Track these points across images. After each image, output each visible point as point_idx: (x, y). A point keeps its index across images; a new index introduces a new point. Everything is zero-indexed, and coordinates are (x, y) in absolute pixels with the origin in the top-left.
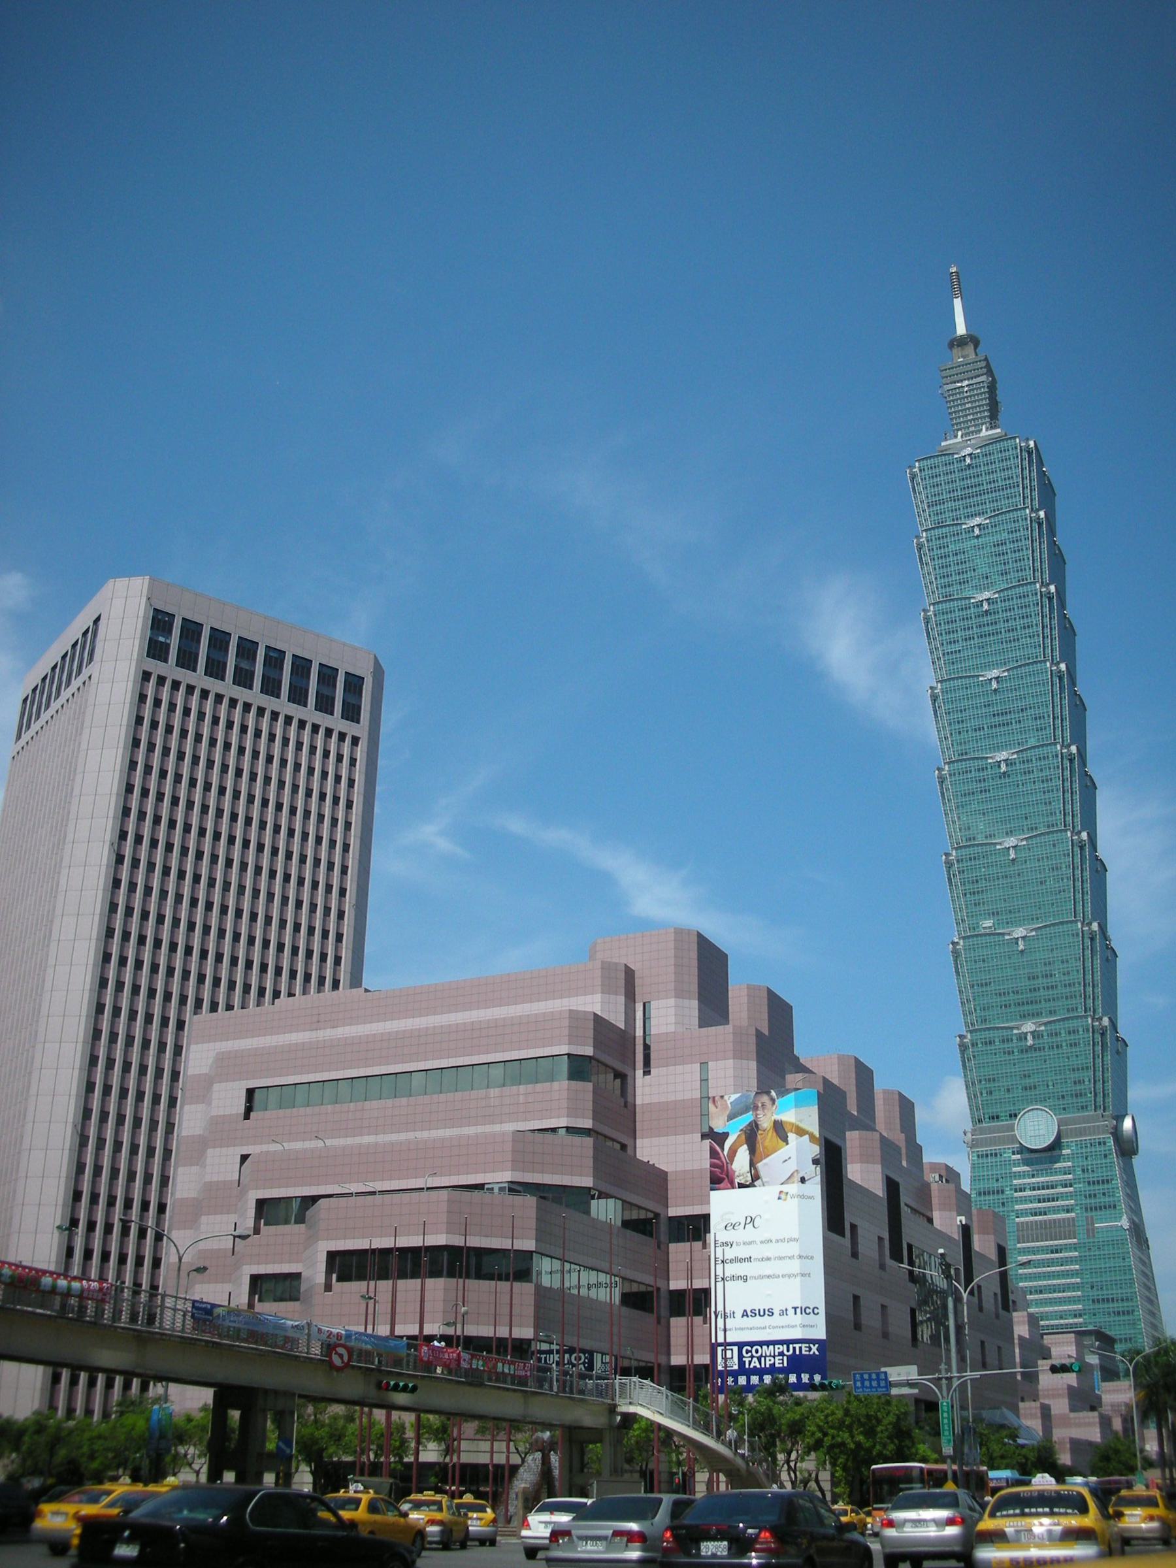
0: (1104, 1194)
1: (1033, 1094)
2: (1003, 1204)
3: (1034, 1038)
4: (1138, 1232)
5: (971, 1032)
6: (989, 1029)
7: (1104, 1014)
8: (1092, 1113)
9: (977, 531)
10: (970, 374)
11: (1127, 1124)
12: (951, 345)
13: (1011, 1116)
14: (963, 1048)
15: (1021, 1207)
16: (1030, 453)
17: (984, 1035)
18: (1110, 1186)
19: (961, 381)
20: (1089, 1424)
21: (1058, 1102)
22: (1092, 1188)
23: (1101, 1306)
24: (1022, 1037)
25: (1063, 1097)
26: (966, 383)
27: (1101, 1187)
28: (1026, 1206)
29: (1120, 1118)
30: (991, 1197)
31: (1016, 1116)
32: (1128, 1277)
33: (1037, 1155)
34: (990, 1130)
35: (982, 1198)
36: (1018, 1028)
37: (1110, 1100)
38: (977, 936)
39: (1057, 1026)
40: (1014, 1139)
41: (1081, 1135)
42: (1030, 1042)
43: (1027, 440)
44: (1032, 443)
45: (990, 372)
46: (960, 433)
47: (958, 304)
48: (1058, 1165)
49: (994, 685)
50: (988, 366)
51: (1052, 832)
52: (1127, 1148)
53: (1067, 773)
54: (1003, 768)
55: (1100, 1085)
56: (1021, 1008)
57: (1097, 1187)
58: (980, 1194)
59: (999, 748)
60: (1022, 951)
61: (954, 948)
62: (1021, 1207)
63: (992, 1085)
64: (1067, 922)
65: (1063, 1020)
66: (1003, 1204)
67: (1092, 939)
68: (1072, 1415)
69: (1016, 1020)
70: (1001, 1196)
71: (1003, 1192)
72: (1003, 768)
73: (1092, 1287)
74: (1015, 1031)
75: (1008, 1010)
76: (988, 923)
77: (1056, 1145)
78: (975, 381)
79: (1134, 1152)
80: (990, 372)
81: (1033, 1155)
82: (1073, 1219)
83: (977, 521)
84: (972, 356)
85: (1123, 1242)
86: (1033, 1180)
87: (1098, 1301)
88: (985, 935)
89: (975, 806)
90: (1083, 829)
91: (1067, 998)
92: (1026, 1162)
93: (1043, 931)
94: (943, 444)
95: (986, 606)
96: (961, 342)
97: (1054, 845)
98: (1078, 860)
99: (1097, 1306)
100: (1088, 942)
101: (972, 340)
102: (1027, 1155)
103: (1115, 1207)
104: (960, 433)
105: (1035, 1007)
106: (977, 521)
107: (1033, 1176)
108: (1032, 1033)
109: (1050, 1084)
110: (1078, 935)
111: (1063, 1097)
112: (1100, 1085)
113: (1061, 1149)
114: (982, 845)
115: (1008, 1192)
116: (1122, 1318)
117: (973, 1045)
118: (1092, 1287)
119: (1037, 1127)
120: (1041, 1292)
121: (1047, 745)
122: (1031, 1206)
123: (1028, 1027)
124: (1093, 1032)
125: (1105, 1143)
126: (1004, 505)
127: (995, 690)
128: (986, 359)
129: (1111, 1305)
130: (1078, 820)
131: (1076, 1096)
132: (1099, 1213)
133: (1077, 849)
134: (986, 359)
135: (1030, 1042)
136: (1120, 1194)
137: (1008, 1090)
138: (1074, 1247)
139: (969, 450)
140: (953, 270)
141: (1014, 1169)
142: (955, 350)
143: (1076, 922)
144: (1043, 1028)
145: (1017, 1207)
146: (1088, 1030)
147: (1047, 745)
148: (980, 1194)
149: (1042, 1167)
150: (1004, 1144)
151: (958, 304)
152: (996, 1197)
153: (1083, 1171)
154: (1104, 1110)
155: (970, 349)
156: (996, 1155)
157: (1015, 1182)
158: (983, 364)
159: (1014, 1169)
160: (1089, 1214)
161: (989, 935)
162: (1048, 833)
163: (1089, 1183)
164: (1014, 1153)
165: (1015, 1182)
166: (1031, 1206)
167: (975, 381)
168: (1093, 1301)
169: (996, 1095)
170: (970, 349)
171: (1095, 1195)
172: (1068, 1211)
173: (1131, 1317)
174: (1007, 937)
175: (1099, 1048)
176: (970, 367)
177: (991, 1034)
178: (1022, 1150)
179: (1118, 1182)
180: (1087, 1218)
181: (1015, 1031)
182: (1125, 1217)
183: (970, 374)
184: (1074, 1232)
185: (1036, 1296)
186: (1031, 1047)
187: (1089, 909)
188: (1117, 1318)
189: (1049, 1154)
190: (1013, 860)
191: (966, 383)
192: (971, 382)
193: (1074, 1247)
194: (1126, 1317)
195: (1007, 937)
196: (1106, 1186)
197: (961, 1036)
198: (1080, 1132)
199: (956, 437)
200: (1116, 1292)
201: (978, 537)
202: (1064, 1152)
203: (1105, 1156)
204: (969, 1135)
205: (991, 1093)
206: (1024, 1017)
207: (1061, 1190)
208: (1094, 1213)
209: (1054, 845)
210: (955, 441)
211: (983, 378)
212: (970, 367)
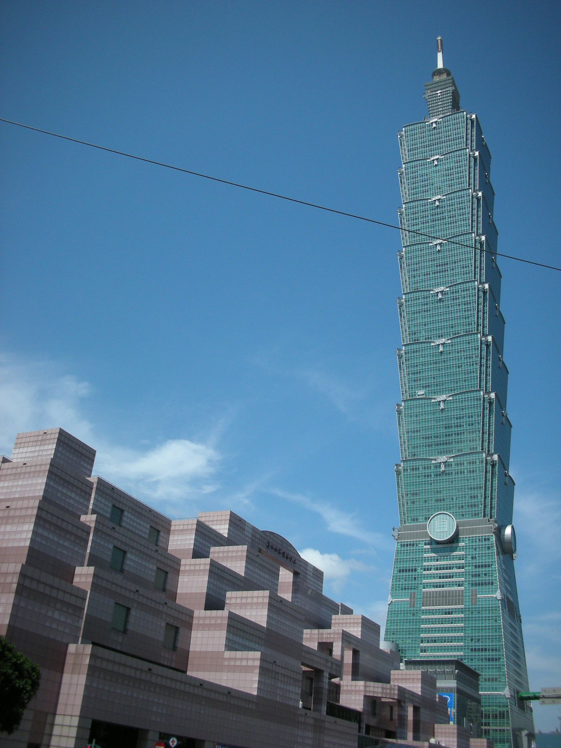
0: (485, 574)
1: (441, 504)
2: (415, 578)
3: (445, 466)
4: (511, 606)
5: (404, 461)
6: (415, 460)
7: (495, 453)
8: (482, 518)
9: (436, 163)
10: (443, 87)
11: (508, 531)
12: (434, 74)
13: (426, 519)
14: (398, 473)
15: (427, 581)
16: (472, 121)
17: (412, 464)
18: (490, 569)
19: (437, 91)
20: (247, 669)
21: (459, 510)
22: (477, 570)
23: (477, 654)
24: (438, 466)
25: (462, 507)
26: (440, 91)
27: (484, 569)
28: (430, 581)
30: (407, 574)
31: (429, 518)
32: (498, 634)
33: (441, 546)
34: (411, 528)
35: (401, 574)
36: (435, 460)
37: (495, 511)
38: (413, 400)
39: (462, 458)
40: (426, 534)
41: (473, 534)
42: (443, 468)
43: (471, 113)
44: (474, 116)
45: (454, 84)
47: (440, 56)
49: (438, 248)
53: (481, 300)
54: (440, 296)
55: (488, 500)
56: (439, 447)
57: (481, 569)
58: (400, 571)
59: (438, 285)
60: (442, 410)
61: (398, 408)
62: (427, 581)
64: (473, 391)
65: (466, 454)
66: (415, 578)
67: (491, 404)
68: (227, 654)
69: (435, 455)
70: (414, 573)
71: (416, 570)
72: (440, 296)
73: (472, 640)
74: (433, 462)
75: (430, 449)
76: (421, 392)
77: (454, 540)
78: (445, 90)
80: (454, 84)
81: (439, 546)
82: (462, 591)
83: (437, 157)
85: (496, 609)
86: (437, 563)
87: (475, 650)
88: (419, 399)
89: (420, 321)
90: (489, 335)
91: (470, 441)
92: (433, 551)
93: (457, 397)
95: (437, 203)
96: (439, 72)
97: (469, 343)
98: (484, 353)
99: (473, 653)
100: (487, 405)
101: (445, 71)
102: (435, 546)
103: (492, 584)
105: (448, 446)
106: (437, 157)
107: (437, 560)
108: (444, 463)
109: (454, 498)
110: (480, 399)
111: (462, 507)
112: (488, 500)
113: (458, 542)
114: (422, 343)
115: (419, 570)
116: (491, 663)
117: (404, 470)
118: (472, 640)
119: (442, 527)
120: (435, 641)
121: (468, 282)
122: (434, 581)
123: (443, 458)
124: (486, 464)
125: (489, 539)
126: (455, 148)
127: (439, 251)
128: (453, 78)
129: (484, 653)
130: (487, 330)
131: (472, 506)
132: (481, 587)
133: (484, 347)
134: (453, 78)
135: (443, 468)
137: (426, 501)
138: (462, 611)
140: (439, 38)
141: (425, 555)
143: (479, 391)
144: (452, 460)
145: (424, 581)
146: (482, 462)
147: (468, 282)
148: (400, 571)
149: (444, 554)
150: (419, 538)
151: (440, 56)
152: (410, 573)
153: (472, 558)
154: (491, 517)
155: (444, 76)
156: (413, 545)
157: (425, 564)
158: (451, 81)
159: (425, 555)
160: (474, 588)
161: (422, 399)
163: (476, 566)
164: (425, 544)
165: (425, 564)
166: (434, 581)
167: (445, 90)
168: (472, 650)
169: (417, 505)
170: (444, 76)
171: (479, 575)
172: (459, 586)
173: (498, 663)
174: (433, 401)
175: (489, 475)
176: (442, 83)
177: (417, 463)
178: (432, 542)
179: (496, 566)
180: (472, 590)
181: (433, 462)
182: (499, 591)
183: (443, 87)
184: (462, 600)
185: (432, 644)
186: (443, 472)
187: (490, 385)
188: (487, 663)
189: (450, 545)
190: (441, 352)
191: (440, 91)
192: (443, 91)
193: (462, 611)
194: (494, 663)
195: (433, 401)
196: (487, 569)
197: (396, 465)
198: (473, 531)
200: (488, 644)
201: (436, 165)
202: (460, 544)
203: (489, 548)
204: (396, 530)
205: (414, 502)
206: (441, 453)
207: (455, 570)
208: (477, 588)
209: (469, 343)
212: (442, 83)
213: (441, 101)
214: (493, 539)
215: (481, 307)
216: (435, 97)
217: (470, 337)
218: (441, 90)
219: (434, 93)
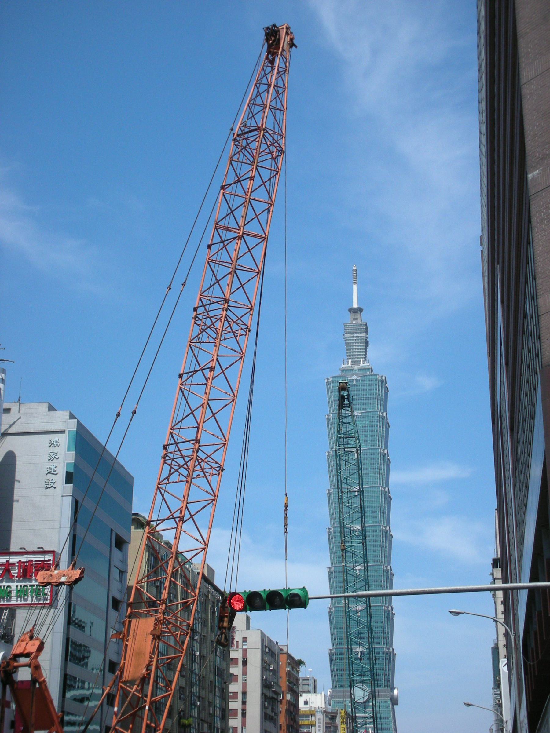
11: (395, 692)
26: (355, 335)
29: (393, 689)
34: (340, 692)
44: (384, 378)
45: (366, 331)
46: (350, 361)
47: (355, 287)
48: (368, 709)
50: (367, 329)
51: (376, 565)
52: (395, 702)
63: (342, 672)
79: (397, 704)
84: (359, 320)
94: (343, 366)
104: (350, 361)
134: (366, 325)
136: (392, 724)
139: (354, 377)
142: (352, 314)
151: (355, 287)
162: (374, 565)
170: (358, 316)
179: (391, 719)
192: (358, 335)
199: (348, 362)
210: (346, 365)
211: (364, 334)
213: (357, 346)
214: (390, 702)
215: (384, 544)
216: (352, 340)
217: (377, 567)
218: (357, 333)
219: (352, 336)
